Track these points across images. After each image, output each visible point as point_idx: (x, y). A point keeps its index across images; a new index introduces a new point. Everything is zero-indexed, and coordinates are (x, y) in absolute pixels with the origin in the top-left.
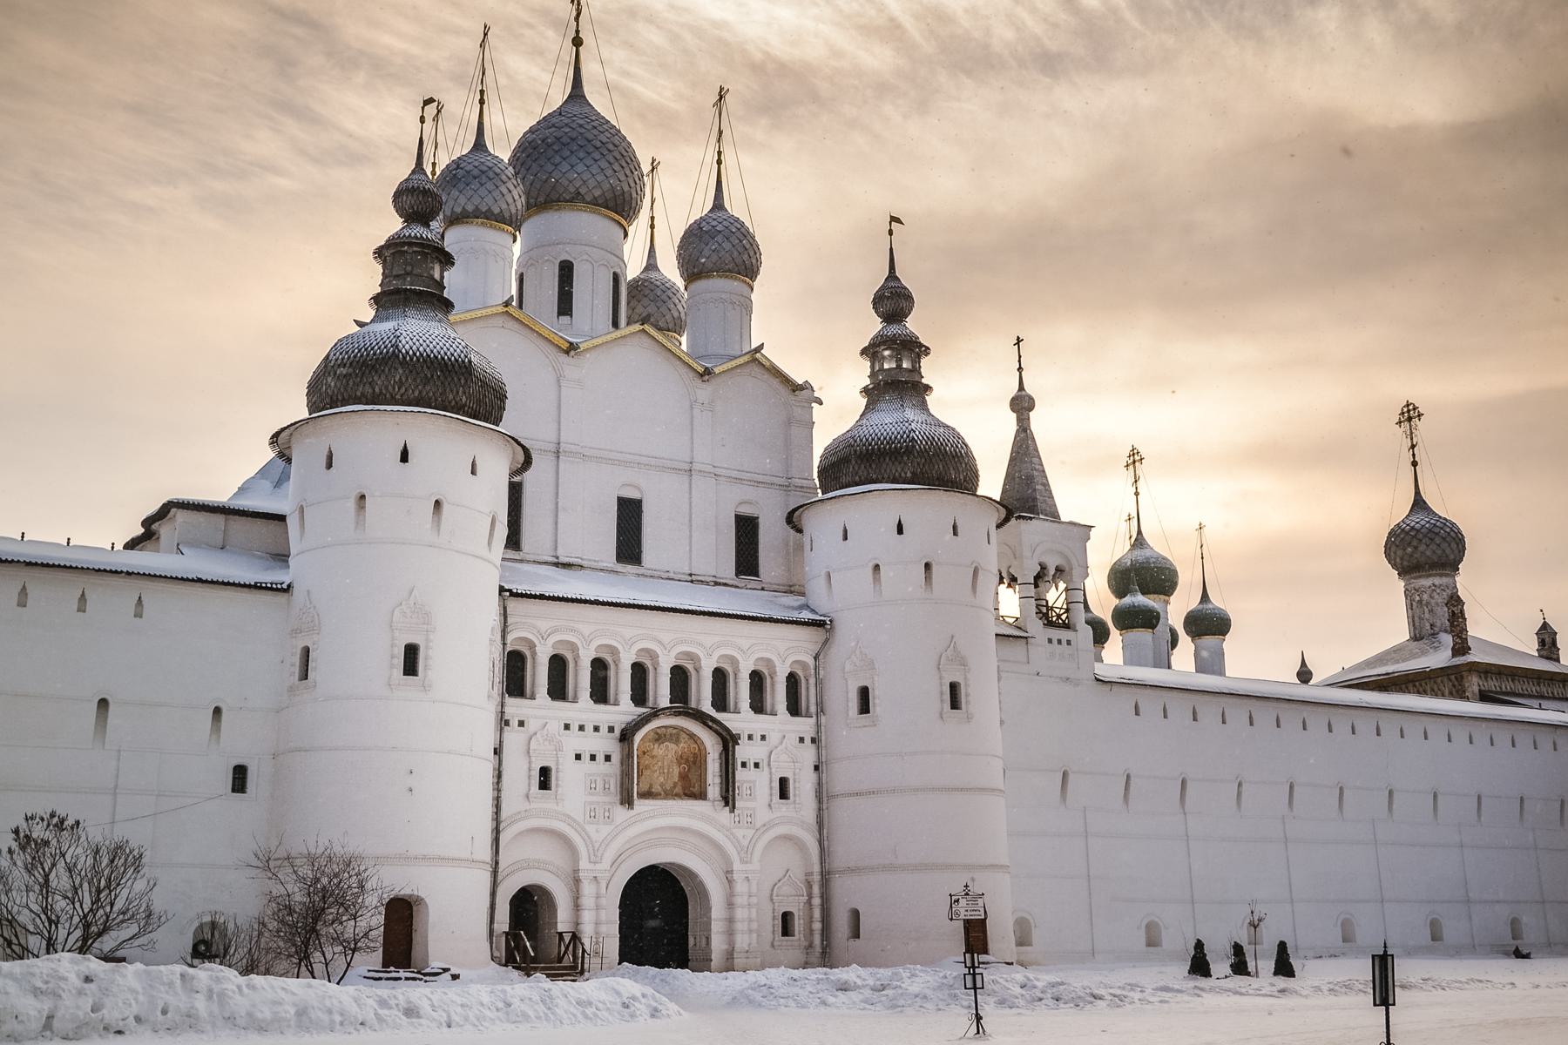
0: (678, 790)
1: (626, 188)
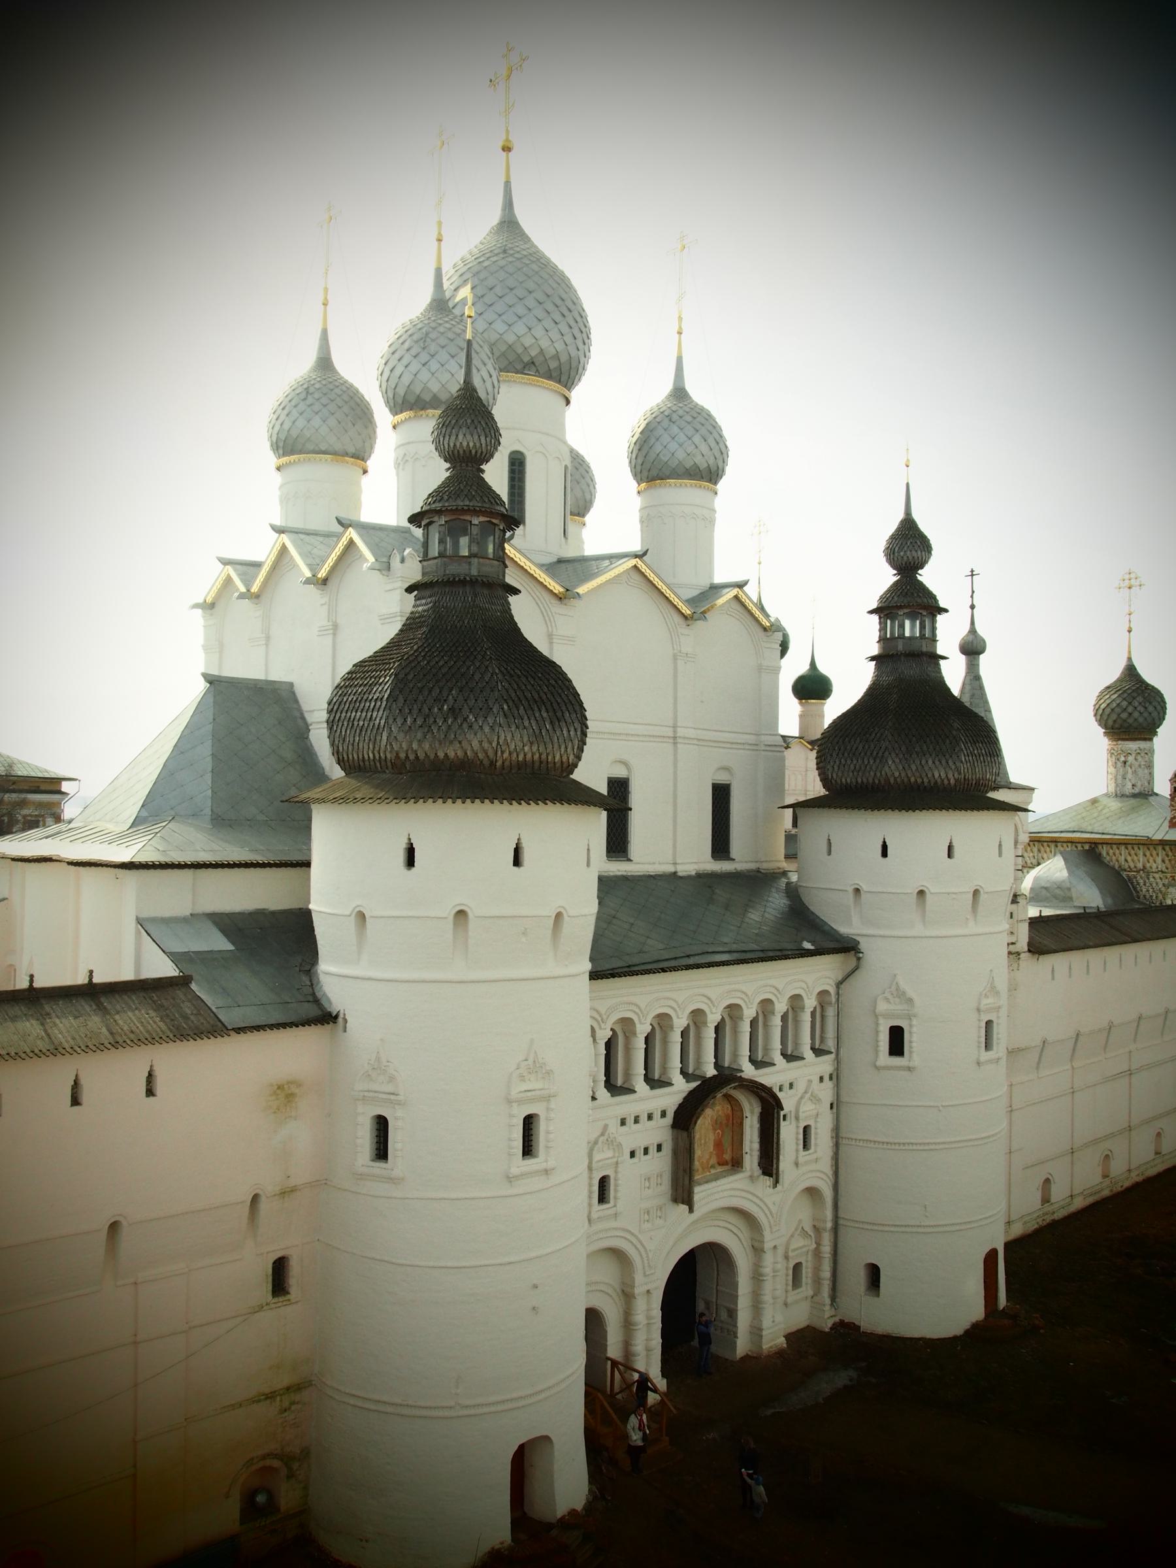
0: (714, 1161)
1: (574, 353)
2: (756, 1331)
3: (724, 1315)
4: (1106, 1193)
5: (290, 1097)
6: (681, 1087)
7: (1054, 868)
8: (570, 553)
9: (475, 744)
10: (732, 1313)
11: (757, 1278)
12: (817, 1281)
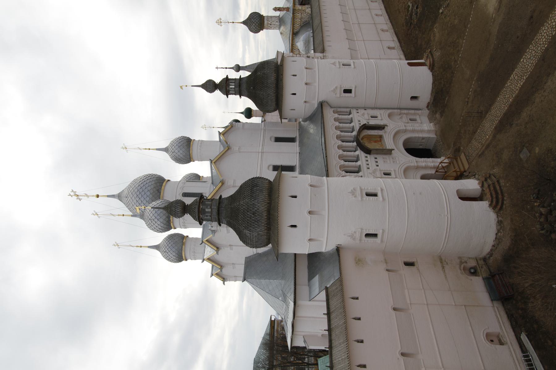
0: (380, 143)
1: (155, 179)
2: (429, 131)
3: (424, 141)
4: (393, 31)
5: (359, 260)
6: (359, 152)
7: (300, 44)
8: (211, 182)
9: (263, 208)
10: (423, 138)
11: (413, 131)
12: (415, 114)
